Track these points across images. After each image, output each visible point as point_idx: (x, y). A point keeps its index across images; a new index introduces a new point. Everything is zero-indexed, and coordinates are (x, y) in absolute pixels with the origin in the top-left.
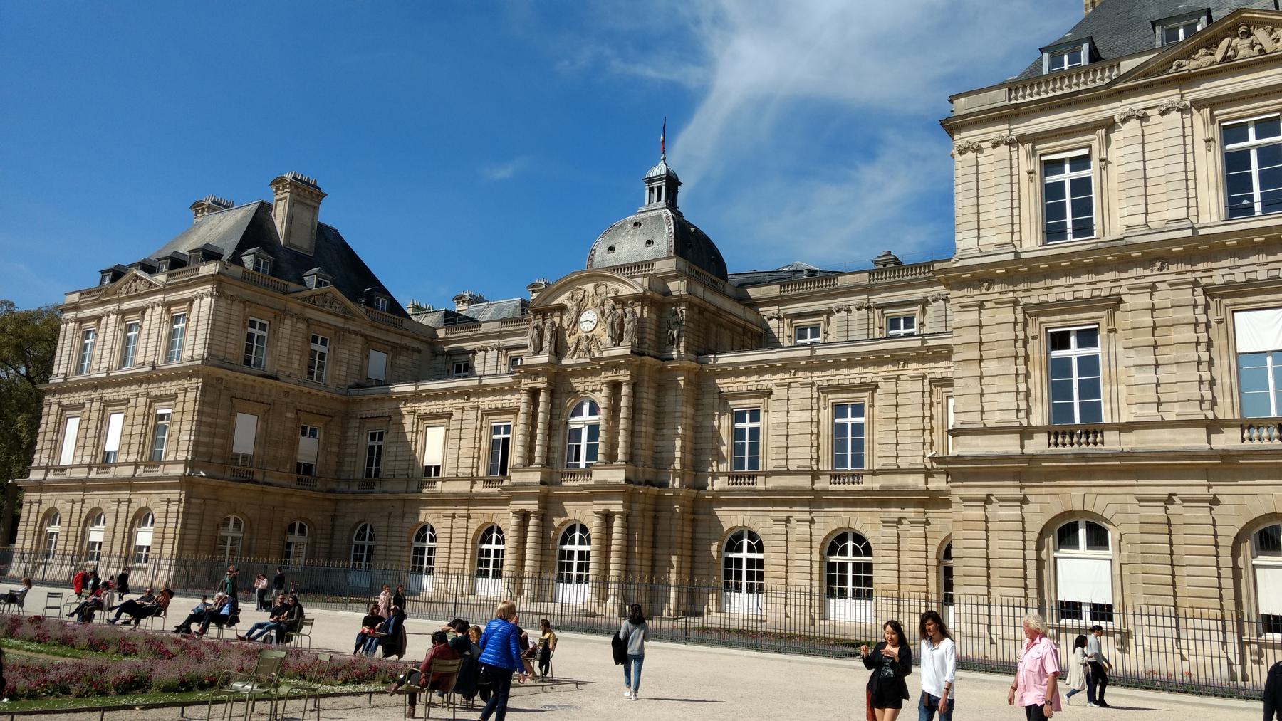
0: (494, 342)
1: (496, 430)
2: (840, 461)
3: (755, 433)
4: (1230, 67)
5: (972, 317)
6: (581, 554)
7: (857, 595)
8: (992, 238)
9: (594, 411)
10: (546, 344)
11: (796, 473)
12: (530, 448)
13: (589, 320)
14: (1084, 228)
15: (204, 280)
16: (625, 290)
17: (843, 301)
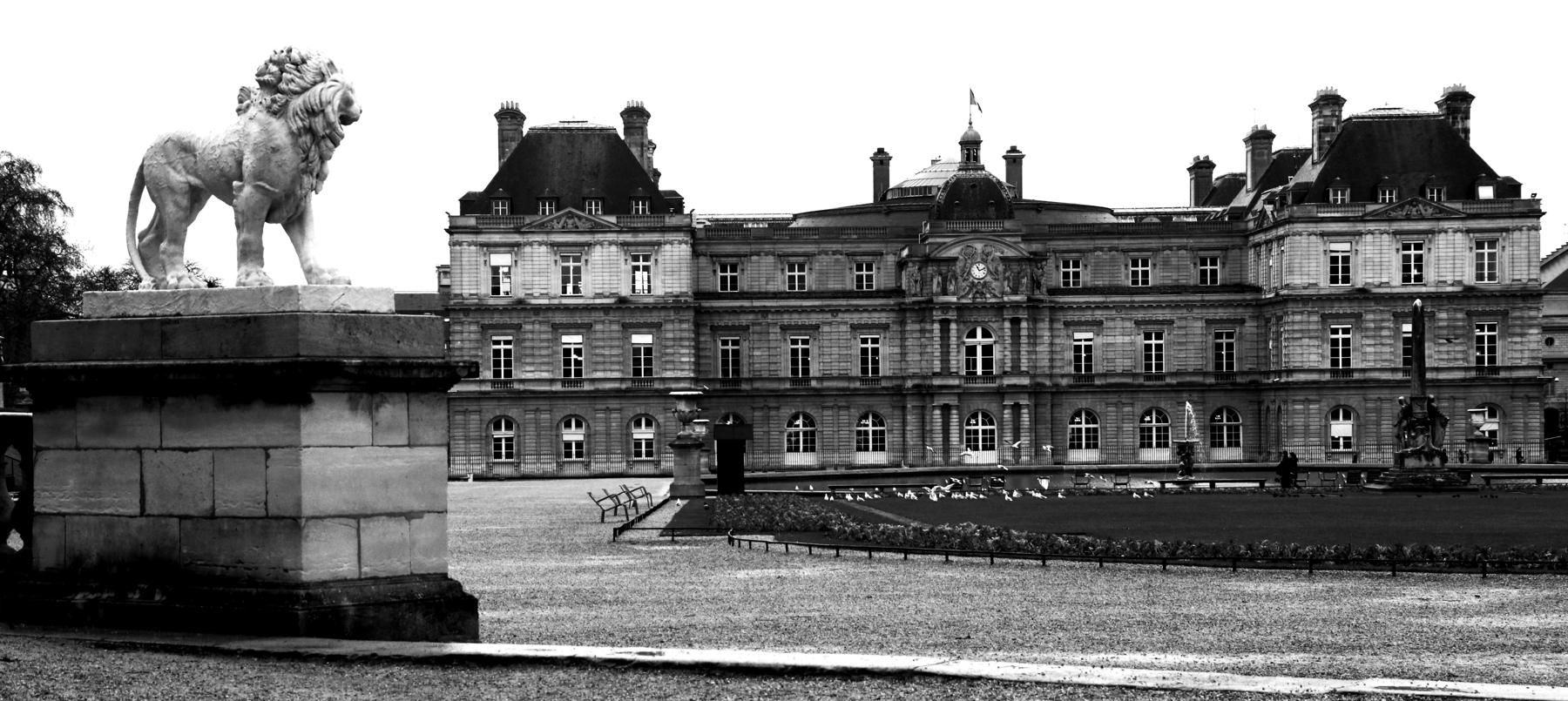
0: (767, 247)
1: (865, 341)
2: (1148, 367)
3: (1088, 349)
4: (1408, 218)
5: (1298, 318)
6: (984, 432)
7: (1158, 445)
8: (1306, 280)
9: (986, 334)
10: (952, 288)
11: (1122, 375)
12: (945, 359)
13: (978, 272)
14: (1346, 280)
15: (677, 229)
16: (1009, 253)
17: (1099, 243)
